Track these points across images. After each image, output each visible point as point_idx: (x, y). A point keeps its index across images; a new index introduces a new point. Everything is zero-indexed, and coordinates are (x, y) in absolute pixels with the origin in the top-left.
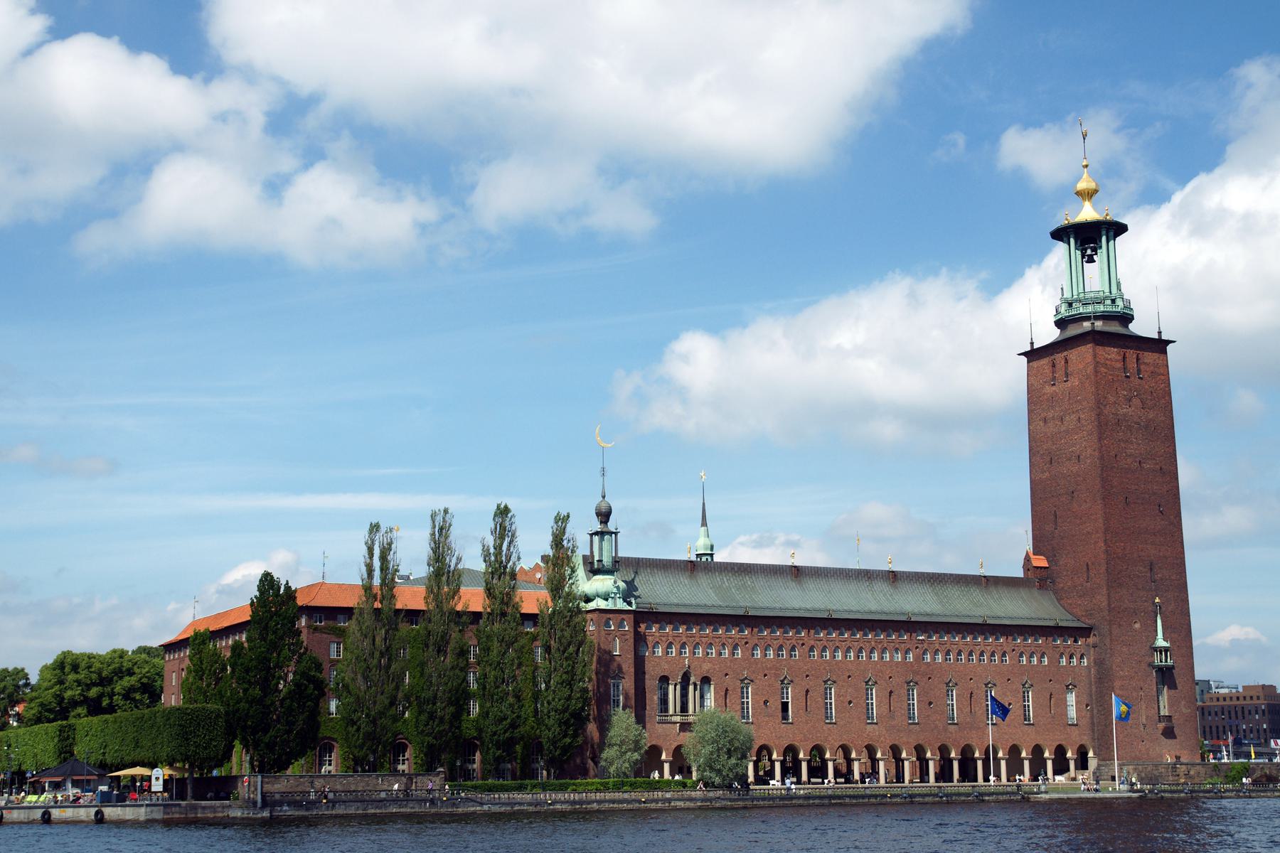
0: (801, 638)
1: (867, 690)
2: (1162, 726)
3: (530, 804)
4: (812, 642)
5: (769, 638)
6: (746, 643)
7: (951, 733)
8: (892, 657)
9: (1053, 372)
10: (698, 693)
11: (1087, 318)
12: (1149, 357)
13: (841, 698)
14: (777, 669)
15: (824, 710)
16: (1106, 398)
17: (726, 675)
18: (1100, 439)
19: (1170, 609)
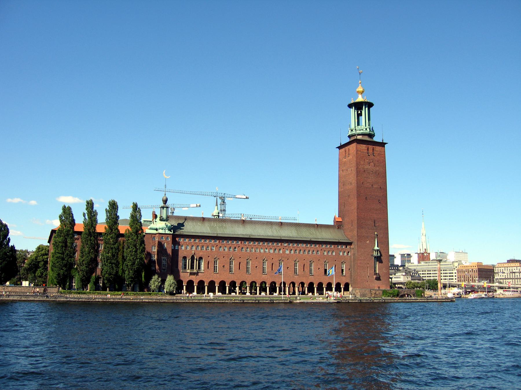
0: (238, 245)
1: (263, 263)
2: (375, 276)
3: (86, 299)
4: (243, 246)
5: (226, 244)
6: (217, 246)
7: (296, 278)
8: (260, 251)
9: (345, 154)
10: (197, 262)
11: (355, 135)
12: (378, 148)
13: (253, 265)
14: (228, 255)
15: (246, 270)
16: (360, 162)
17: (209, 256)
18: (357, 177)
19: (381, 236)
